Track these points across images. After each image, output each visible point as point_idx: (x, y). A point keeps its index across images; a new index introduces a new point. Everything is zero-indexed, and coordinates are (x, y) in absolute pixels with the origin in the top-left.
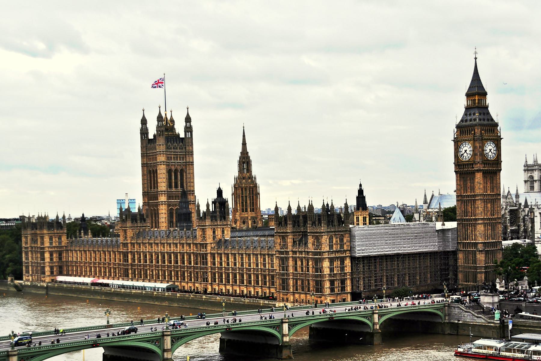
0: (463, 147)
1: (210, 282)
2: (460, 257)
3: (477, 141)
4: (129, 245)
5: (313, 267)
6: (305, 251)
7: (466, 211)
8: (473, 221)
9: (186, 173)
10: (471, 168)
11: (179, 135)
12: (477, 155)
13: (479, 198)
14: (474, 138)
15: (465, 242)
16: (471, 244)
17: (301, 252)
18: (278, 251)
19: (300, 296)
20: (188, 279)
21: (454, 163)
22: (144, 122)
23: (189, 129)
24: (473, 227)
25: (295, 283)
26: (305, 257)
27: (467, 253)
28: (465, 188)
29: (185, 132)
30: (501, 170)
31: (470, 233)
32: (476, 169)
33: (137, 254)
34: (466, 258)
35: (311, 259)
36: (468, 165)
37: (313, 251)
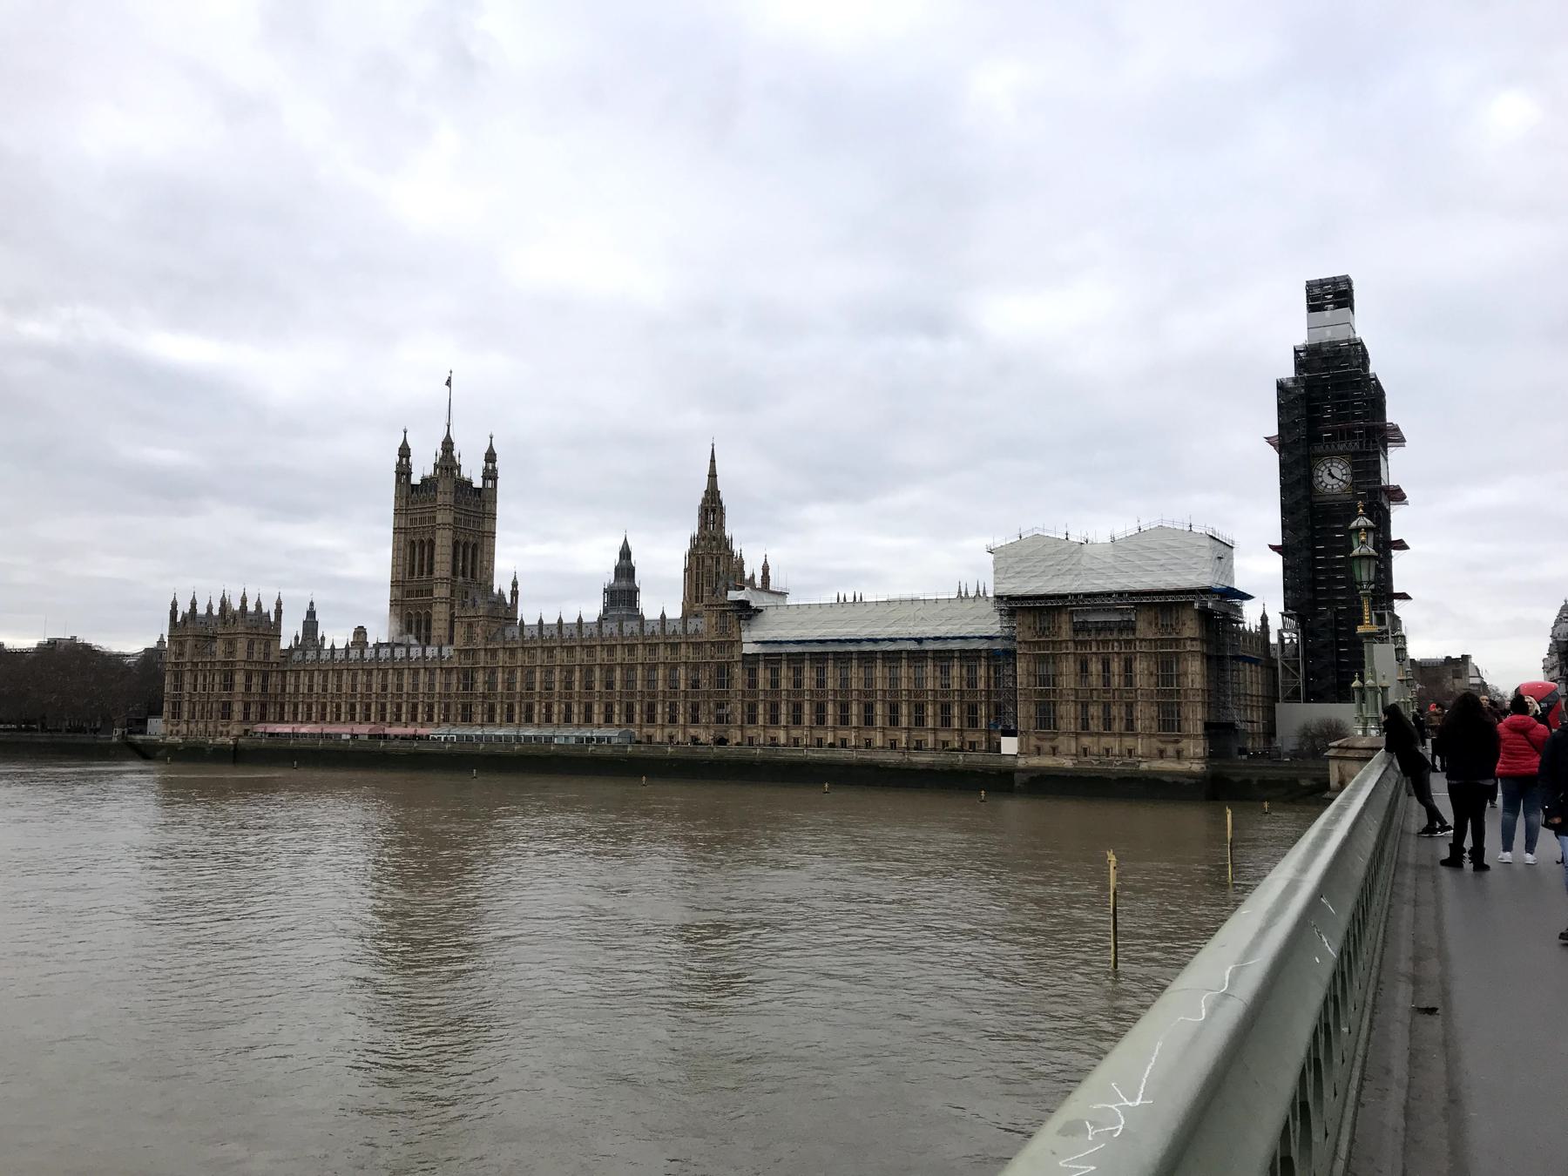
0: (1322, 469)
1: (739, 723)
4: (483, 653)
5: (1152, 674)
6: (1118, 641)
9: (482, 551)
11: (470, 483)
17: (1105, 642)
18: (1026, 642)
19: (1098, 741)
20: (663, 718)
22: (405, 452)
23: (490, 475)
25: (1079, 713)
26: (1118, 653)
29: (485, 478)
33: (503, 673)
35: (1146, 657)
37: (1150, 636)
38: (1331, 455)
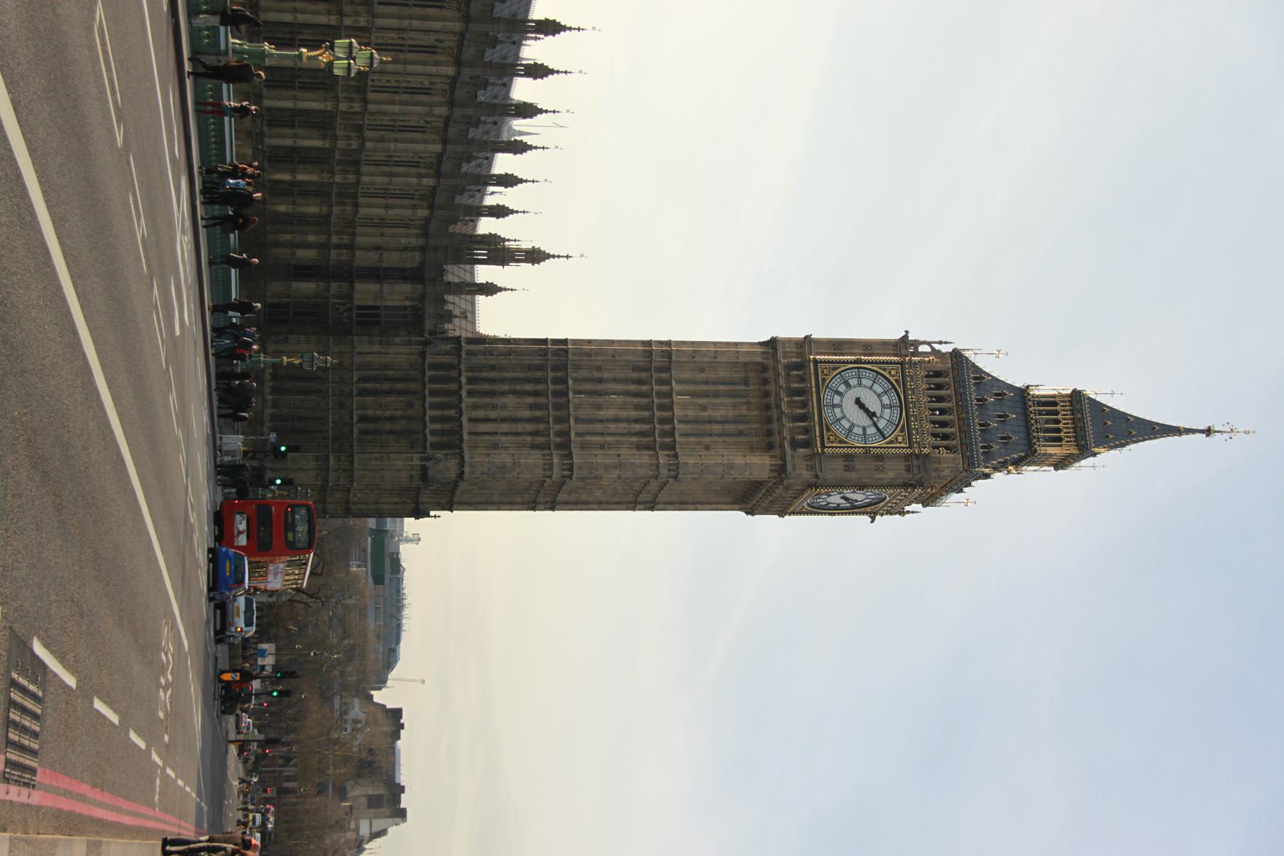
0: (876, 387)
2: (391, 350)
3: (908, 469)
7: (599, 387)
8: (558, 427)
10: (792, 430)
12: (847, 469)
13: (664, 471)
14: (917, 456)
15: (463, 380)
16: (452, 413)
21: (806, 337)
24: (529, 427)
27: (412, 386)
28: (705, 388)
30: (751, 512)
31: (505, 407)
32: (789, 458)
34: (387, 379)
36: (803, 418)
38: (904, 405)
